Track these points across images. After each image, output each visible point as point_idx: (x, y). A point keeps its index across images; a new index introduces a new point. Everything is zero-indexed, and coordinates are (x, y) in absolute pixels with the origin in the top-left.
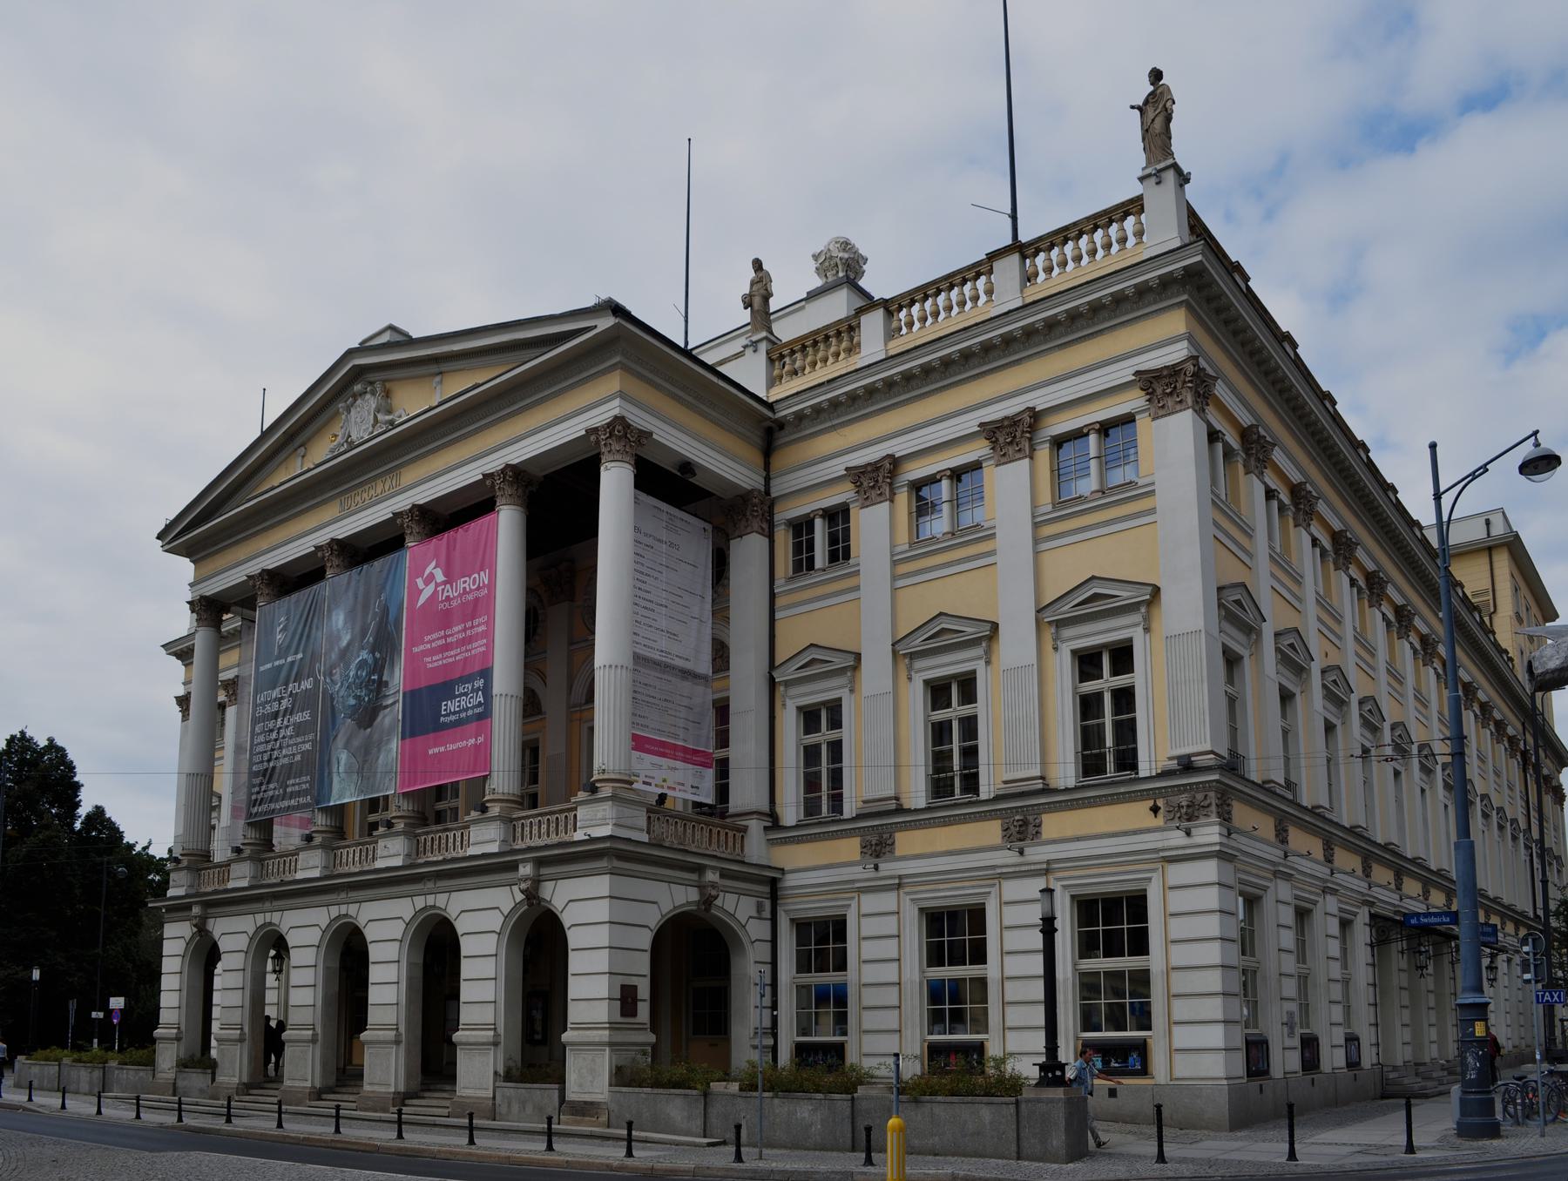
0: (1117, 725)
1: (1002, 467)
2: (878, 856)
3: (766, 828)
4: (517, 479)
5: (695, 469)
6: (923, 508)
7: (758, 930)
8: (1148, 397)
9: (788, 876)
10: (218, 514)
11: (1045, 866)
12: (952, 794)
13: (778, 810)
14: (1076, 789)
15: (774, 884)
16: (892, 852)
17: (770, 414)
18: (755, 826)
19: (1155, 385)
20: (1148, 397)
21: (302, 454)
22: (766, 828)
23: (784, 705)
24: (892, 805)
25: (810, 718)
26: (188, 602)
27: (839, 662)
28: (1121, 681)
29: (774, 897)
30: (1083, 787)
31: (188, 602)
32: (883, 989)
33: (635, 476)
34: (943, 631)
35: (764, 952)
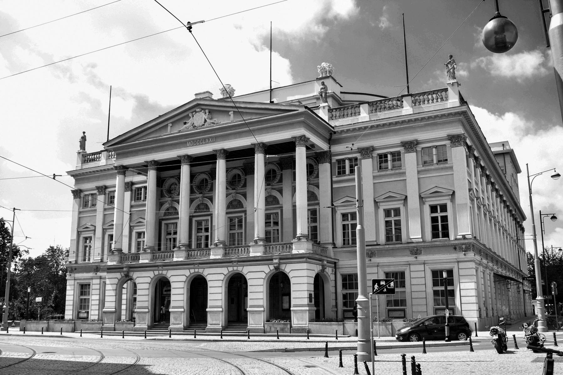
0: (442, 225)
2: (371, 257)
3: (333, 248)
7: (332, 277)
9: (340, 262)
12: (392, 240)
13: (335, 242)
14: (431, 242)
15: (335, 263)
17: (333, 130)
18: (330, 247)
22: (333, 248)
24: (375, 243)
28: (444, 214)
29: (335, 267)
35: (333, 284)
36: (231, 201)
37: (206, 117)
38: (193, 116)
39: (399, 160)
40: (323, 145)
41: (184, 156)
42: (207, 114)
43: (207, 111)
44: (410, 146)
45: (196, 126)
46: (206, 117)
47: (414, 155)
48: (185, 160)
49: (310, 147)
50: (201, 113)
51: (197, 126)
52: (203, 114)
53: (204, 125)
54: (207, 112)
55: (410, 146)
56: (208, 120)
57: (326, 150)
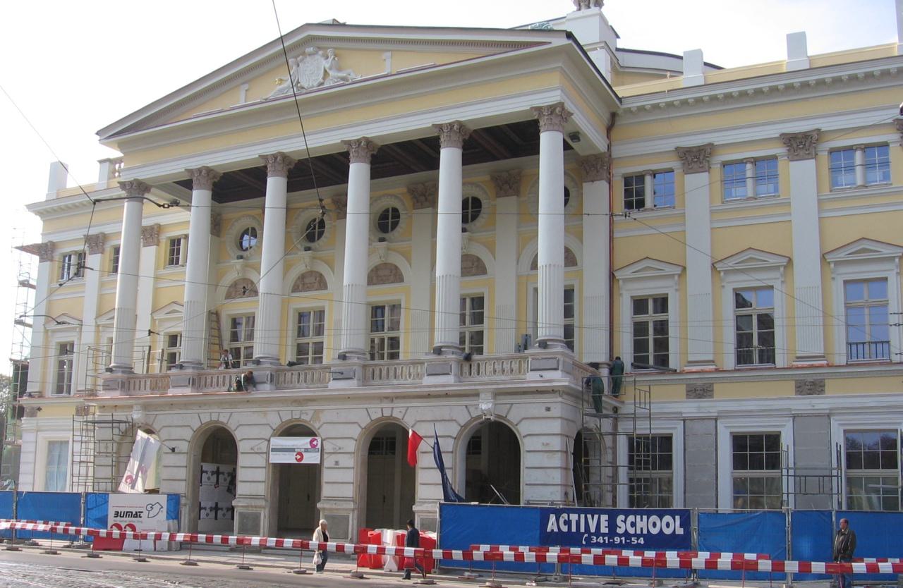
1: (795, 162)
4: (208, 175)
5: (580, 135)
6: (728, 182)
8: (788, 148)
10: (145, 127)
11: (828, 411)
16: (711, 396)
19: (792, 142)
20: (788, 148)
21: (246, 89)
23: (621, 295)
25: (639, 305)
26: (33, 208)
27: (669, 270)
30: (738, 370)
31: (33, 208)
32: (535, 487)
33: (288, 183)
34: (751, 259)
36: (376, 267)
37: (327, 66)
38: (298, 66)
39: (773, 177)
40: (595, 138)
41: (275, 156)
42: (330, 59)
43: (330, 52)
44: (800, 144)
45: (303, 88)
46: (327, 66)
47: (810, 164)
48: (276, 165)
49: (571, 141)
50: (317, 57)
51: (306, 86)
52: (322, 59)
53: (322, 84)
54: (329, 54)
55: (800, 144)
56: (331, 73)
57: (603, 151)
